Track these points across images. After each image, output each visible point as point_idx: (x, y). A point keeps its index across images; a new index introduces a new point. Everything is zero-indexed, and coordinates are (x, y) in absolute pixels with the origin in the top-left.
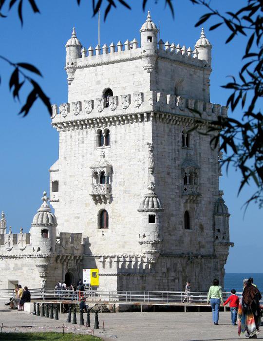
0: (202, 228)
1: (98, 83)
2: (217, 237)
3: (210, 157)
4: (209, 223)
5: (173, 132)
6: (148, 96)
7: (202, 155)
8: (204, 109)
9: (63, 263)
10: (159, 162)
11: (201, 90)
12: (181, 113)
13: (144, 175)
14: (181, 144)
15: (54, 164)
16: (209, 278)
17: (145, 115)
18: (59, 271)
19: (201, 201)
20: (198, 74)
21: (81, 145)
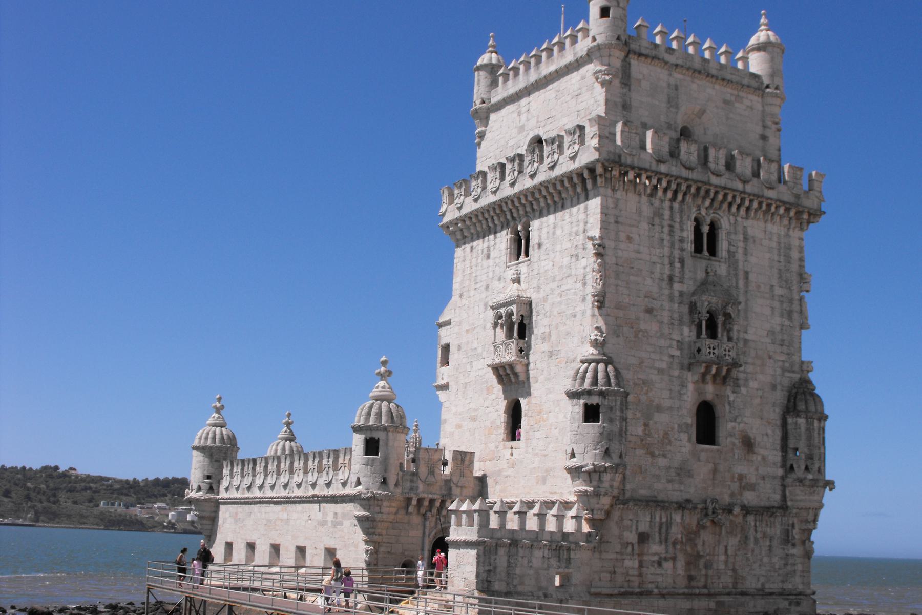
0: (748, 444)
1: (522, 129)
2: (792, 467)
3: (775, 282)
4: (770, 432)
6: (591, 130)
7: (752, 277)
8: (756, 174)
9: (424, 515)
10: (620, 283)
11: (757, 137)
12: (685, 173)
13: (584, 313)
14: (690, 247)
15: (446, 310)
16: (766, 560)
17: (586, 175)
18: (416, 533)
19: (746, 380)
21: (485, 263)
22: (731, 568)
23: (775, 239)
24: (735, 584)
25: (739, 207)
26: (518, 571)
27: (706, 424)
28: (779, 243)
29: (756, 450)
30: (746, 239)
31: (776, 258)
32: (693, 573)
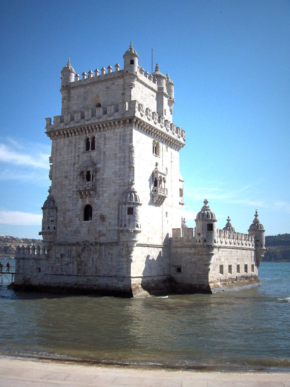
0: (103, 218)
3: (117, 152)
5: (74, 142)
11: (120, 95)
16: (110, 263)
19: (103, 194)
20: (116, 84)
22: (94, 265)
23: (118, 134)
24: (96, 272)
25: (100, 128)
26: (26, 267)
27: (88, 212)
28: (120, 136)
29: (106, 220)
30: (105, 139)
31: (118, 142)
32: (80, 268)
